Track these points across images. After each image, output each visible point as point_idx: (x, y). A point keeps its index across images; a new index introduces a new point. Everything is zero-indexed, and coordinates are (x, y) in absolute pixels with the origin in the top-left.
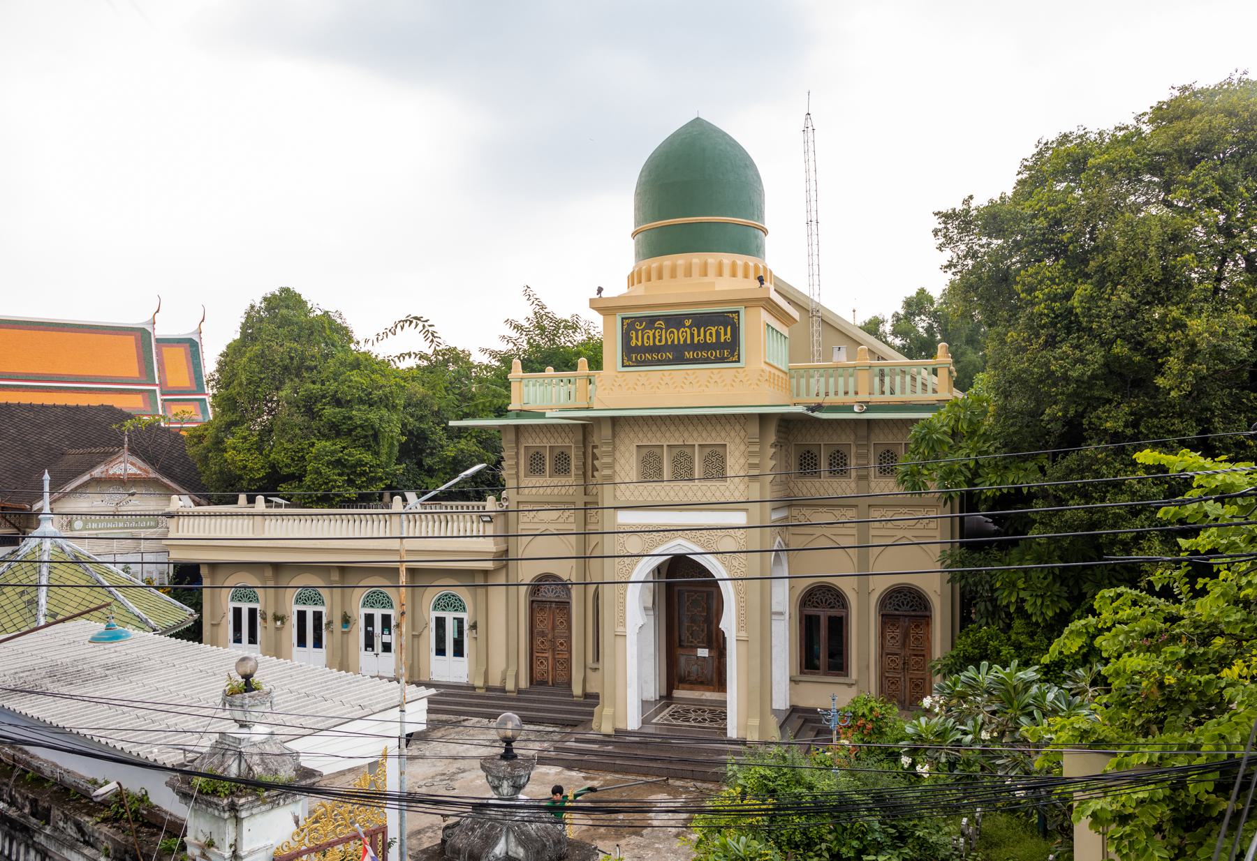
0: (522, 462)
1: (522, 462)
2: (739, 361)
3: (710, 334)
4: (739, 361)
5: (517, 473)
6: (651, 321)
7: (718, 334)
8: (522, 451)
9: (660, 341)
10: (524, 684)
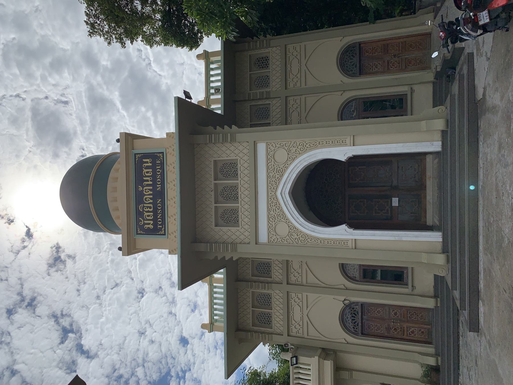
0: (263, 329)
1: (263, 329)
2: (163, 153)
3: (147, 172)
4: (163, 153)
5: (269, 333)
6: (139, 214)
7: (147, 168)
8: (256, 328)
9: (150, 208)
10: (431, 350)
